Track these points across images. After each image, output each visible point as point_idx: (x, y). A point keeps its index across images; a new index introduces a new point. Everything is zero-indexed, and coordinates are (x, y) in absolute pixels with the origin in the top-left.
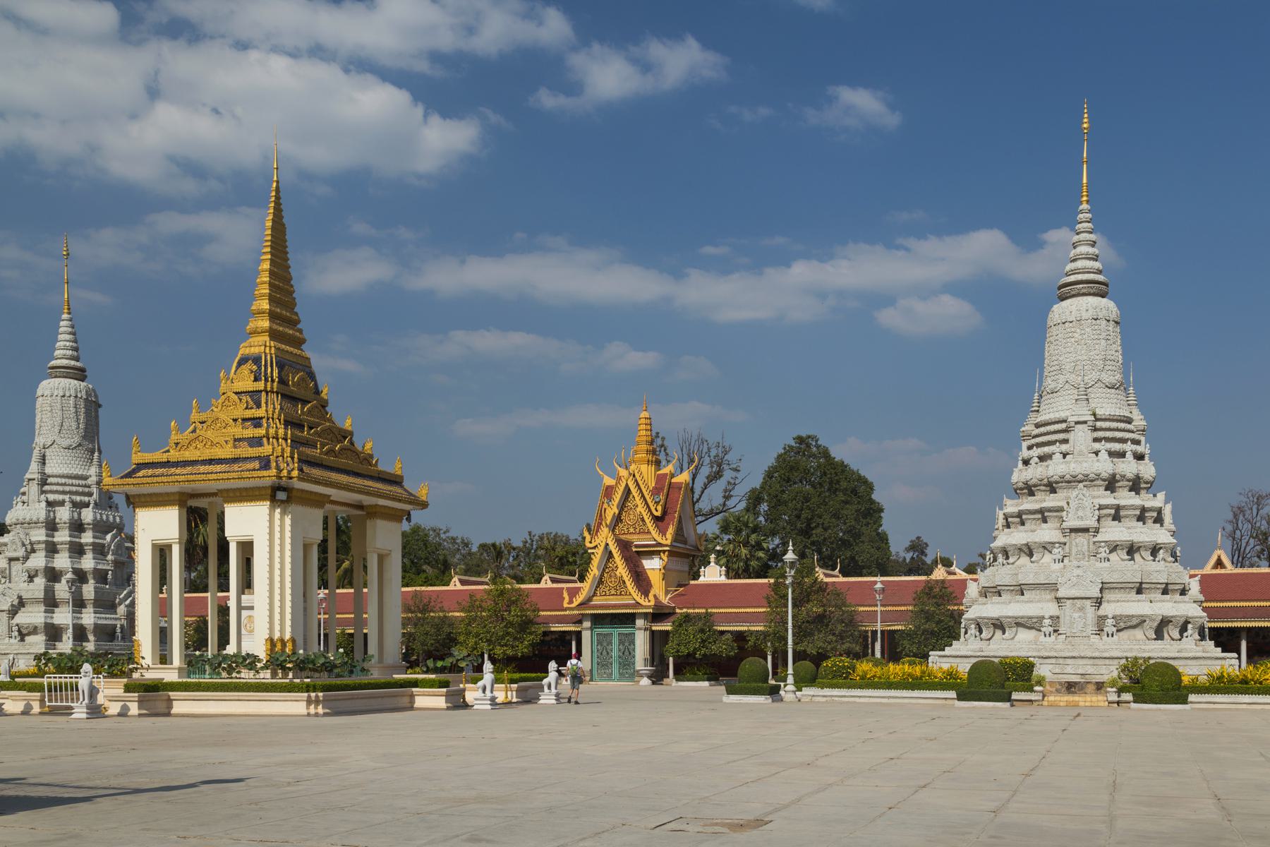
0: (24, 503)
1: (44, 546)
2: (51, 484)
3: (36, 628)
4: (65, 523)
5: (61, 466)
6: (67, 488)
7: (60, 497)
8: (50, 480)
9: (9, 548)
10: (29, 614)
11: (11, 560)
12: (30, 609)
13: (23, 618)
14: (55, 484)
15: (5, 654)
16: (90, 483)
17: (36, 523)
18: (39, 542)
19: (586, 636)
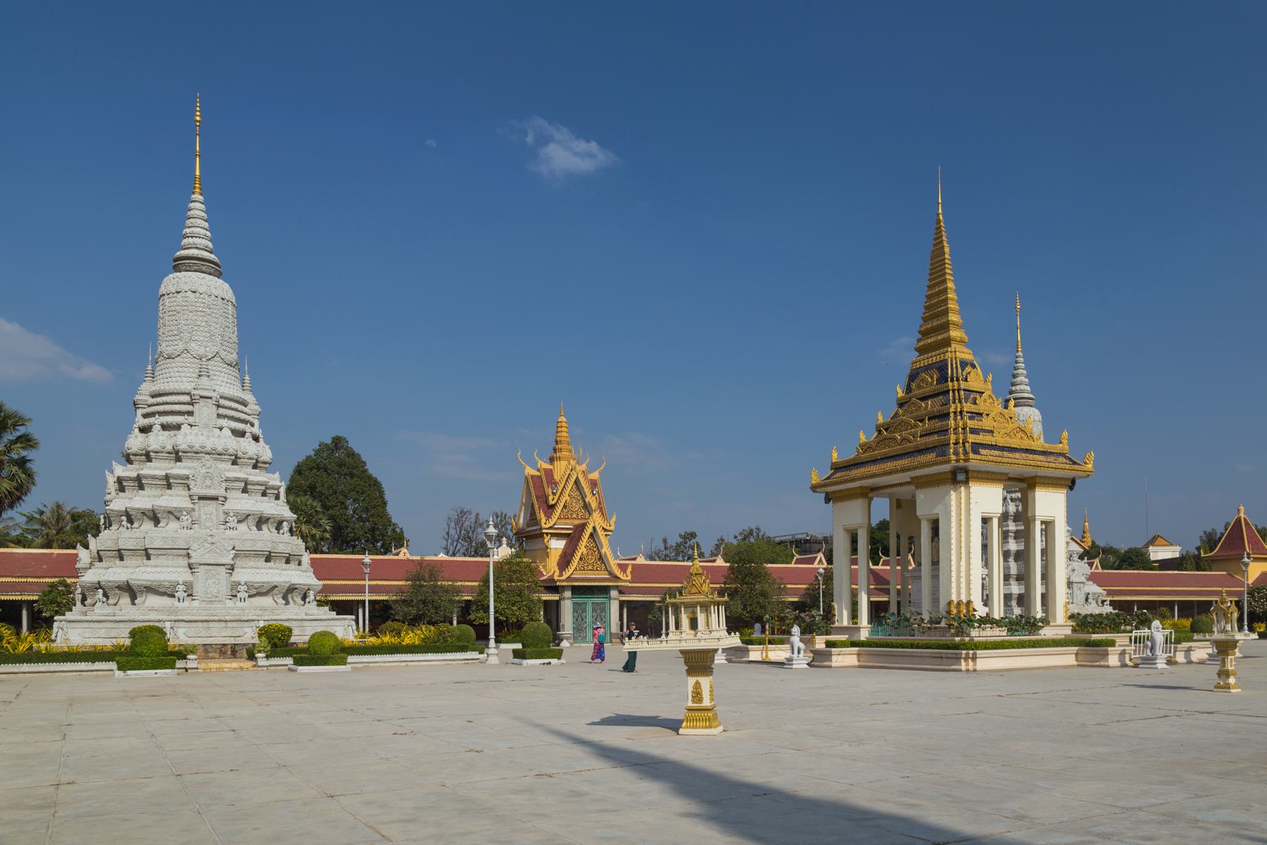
0: (191, 426)
1: (243, 484)
2: (223, 407)
3: (277, 587)
4: (251, 459)
5: (228, 385)
6: (243, 416)
7: (240, 426)
8: (222, 402)
9: (198, 483)
10: (258, 571)
11: (201, 498)
12: (251, 564)
13: (242, 575)
14: (226, 408)
15: (247, 621)
16: (248, 411)
17: (220, 454)
18: (237, 480)
19: (567, 608)
